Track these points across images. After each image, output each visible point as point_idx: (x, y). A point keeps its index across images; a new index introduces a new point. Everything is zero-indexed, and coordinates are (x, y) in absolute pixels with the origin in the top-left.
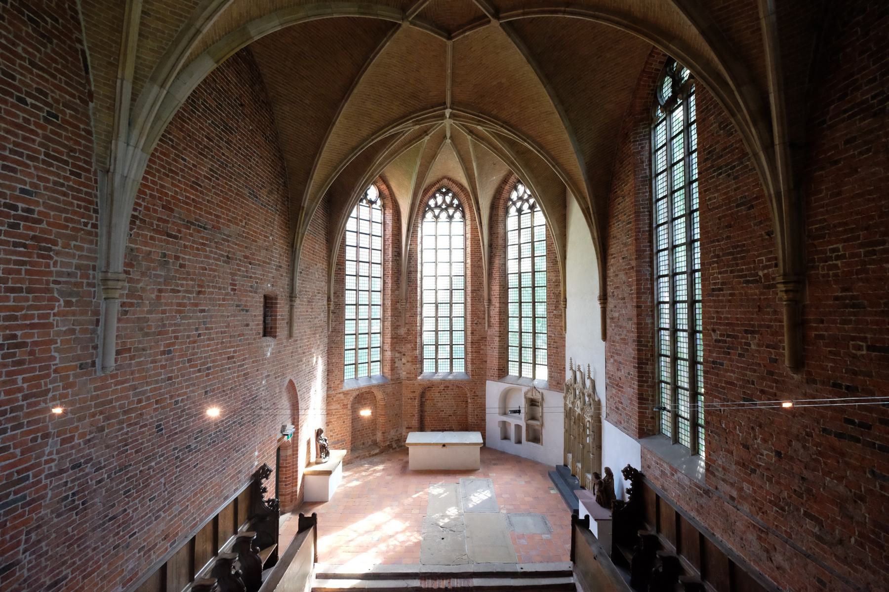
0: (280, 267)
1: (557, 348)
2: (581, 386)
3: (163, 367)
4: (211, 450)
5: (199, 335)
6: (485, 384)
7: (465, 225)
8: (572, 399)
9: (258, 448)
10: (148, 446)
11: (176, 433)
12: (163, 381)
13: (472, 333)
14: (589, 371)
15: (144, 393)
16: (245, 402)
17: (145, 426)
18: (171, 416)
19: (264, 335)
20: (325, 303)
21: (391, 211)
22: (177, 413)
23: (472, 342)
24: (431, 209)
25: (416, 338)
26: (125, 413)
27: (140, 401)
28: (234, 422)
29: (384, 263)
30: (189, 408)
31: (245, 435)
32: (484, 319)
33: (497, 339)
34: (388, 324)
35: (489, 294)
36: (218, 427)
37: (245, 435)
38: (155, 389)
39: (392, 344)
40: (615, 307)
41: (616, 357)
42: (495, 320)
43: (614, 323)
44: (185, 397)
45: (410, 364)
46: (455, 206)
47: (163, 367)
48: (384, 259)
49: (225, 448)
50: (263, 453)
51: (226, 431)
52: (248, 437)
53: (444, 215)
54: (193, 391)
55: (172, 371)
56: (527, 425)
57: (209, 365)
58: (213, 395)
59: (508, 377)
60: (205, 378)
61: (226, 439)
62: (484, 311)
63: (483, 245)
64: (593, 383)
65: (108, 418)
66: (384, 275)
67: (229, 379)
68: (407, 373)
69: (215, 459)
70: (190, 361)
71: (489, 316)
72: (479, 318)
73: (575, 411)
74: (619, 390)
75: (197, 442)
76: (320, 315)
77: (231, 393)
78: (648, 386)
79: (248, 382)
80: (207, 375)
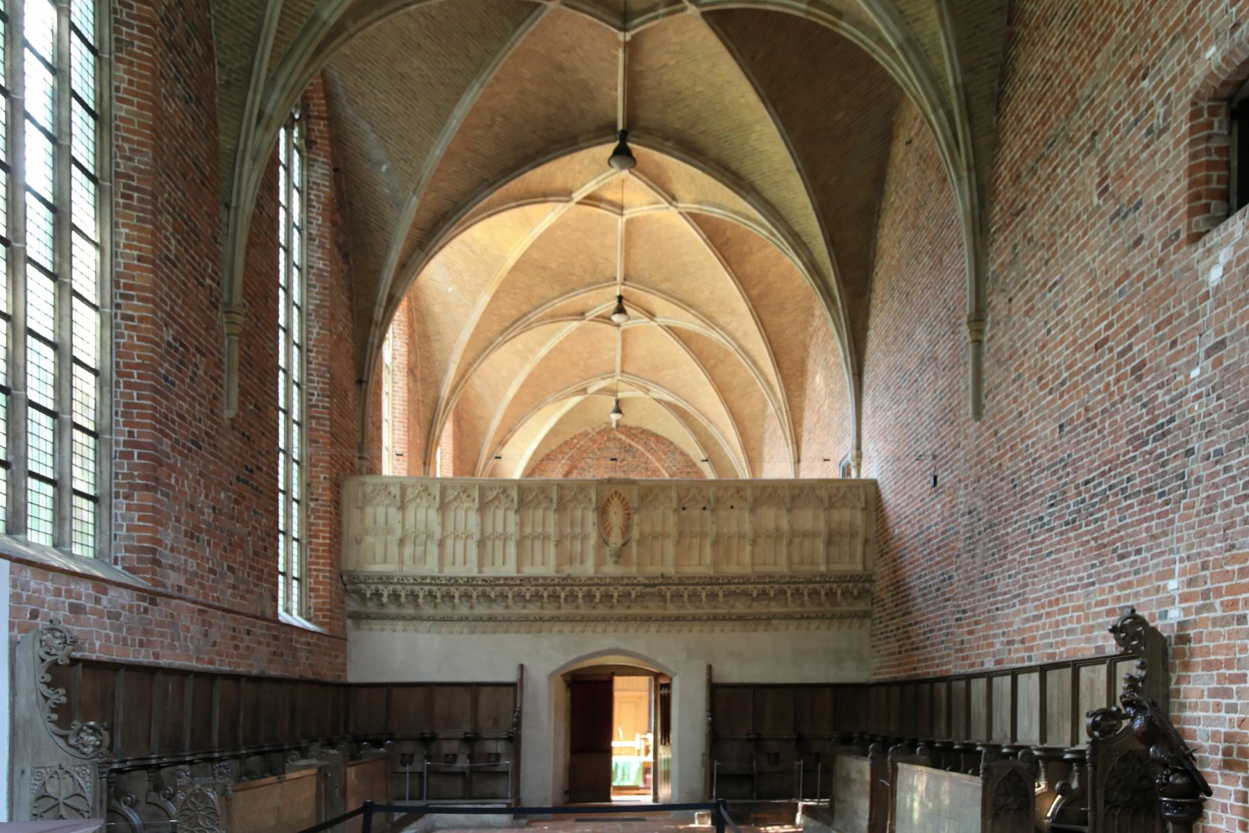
16: (1138, 441)
28: (1111, 488)
30: (1040, 457)
49: (1096, 539)
51: (1093, 505)
77: (1103, 421)
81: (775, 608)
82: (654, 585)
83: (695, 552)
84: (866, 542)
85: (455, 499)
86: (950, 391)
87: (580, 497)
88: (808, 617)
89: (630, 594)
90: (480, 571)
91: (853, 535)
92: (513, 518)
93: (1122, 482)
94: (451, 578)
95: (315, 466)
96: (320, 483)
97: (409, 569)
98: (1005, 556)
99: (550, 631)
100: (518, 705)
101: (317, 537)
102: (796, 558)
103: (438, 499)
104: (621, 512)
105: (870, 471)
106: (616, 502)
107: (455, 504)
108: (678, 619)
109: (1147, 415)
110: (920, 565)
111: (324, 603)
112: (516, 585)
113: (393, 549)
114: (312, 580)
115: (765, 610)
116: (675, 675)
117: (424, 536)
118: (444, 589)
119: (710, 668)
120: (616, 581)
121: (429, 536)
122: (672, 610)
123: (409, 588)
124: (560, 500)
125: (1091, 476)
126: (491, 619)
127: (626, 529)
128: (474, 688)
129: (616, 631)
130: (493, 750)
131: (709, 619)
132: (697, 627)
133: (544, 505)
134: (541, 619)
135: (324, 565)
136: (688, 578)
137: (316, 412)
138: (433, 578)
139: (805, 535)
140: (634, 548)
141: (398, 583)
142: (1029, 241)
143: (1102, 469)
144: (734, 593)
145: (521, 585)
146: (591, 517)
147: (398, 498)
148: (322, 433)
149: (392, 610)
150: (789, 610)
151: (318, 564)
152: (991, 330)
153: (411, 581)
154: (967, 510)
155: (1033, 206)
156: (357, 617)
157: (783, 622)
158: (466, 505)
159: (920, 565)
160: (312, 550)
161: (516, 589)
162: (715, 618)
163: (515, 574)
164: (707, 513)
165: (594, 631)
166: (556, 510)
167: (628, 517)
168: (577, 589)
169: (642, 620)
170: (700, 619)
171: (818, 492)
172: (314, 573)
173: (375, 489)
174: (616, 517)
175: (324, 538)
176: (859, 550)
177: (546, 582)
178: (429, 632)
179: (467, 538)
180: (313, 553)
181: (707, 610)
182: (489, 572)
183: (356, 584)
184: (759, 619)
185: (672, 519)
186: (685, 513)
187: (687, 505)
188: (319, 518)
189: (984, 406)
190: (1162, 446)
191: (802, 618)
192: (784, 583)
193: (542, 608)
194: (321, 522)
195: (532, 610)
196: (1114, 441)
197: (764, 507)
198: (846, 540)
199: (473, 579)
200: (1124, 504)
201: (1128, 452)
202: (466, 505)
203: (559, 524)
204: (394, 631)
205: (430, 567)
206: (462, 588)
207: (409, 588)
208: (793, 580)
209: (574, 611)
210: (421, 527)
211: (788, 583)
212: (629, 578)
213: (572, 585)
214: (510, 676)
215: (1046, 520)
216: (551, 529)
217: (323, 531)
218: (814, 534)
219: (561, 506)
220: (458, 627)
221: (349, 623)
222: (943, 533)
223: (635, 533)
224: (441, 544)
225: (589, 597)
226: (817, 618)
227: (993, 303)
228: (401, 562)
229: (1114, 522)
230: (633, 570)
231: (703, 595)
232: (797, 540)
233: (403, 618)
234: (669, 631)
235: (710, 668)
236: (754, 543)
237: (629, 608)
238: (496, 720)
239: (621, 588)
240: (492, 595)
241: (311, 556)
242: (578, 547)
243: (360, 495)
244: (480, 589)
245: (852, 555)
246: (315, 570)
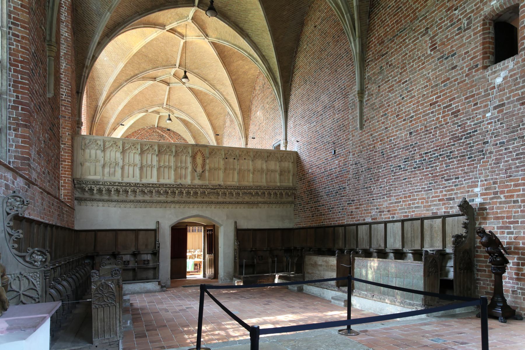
10: (378, 162)
11: (392, 157)
12: (383, 130)
15: (375, 137)
17: (376, 152)
18: (388, 148)
26: (369, 145)
27: (373, 141)
38: (380, 134)
44: (396, 137)
54: (400, 133)
55: (388, 124)
60: (409, 124)
65: (363, 148)
70: (397, 116)
75: (405, 165)
80: (411, 122)
81: (260, 199)
82: (215, 189)
83: (231, 176)
84: (293, 175)
85: (129, 148)
86: (343, 119)
87: (185, 151)
88: (272, 203)
89: (205, 192)
90: (141, 181)
91: (289, 172)
92: (155, 158)
94: (127, 183)
95: (64, 128)
96: (67, 136)
97: (107, 178)
98: (378, 180)
99: (170, 207)
100: (157, 239)
101: (65, 162)
102: (269, 180)
103: (121, 148)
104: (201, 158)
105: (293, 147)
106: (199, 154)
107: (129, 151)
108: (223, 203)
110: (326, 183)
111: (68, 193)
112: (157, 187)
113: (99, 169)
114: (62, 182)
115: (256, 200)
116: (221, 225)
117: (114, 164)
118: (124, 188)
119: (236, 223)
120: (201, 186)
121: (117, 164)
122: (221, 199)
123: (107, 187)
124: (176, 152)
126: (144, 202)
127: (203, 166)
128: (136, 231)
129: (198, 207)
130: (146, 259)
131: (235, 203)
132: (230, 206)
133: (169, 154)
134: (167, 202)
135: (68, 174)
136: (229, 186)
137: (64, 103)
138: (119, 183)
139: (272, 171)
140: (207, 174)
141: (102, 185)
142: (390, 66)
144: (246, 193)
145: (159, 187)
146: (189, 160)
147: (102, 146)
148: (67, 113)
149: (98, 197)
150: (265, 200)
151: (65, 174)
152: (368, 97)
153: (109, 184)
154: (354, 163)
155: (392, 53)
156: (80, 200)
157: (263, 205)
158: (134, 151)
159: (326, 183)
160: (62, 167)
161: (156, 189)
162: (238, 203)
163: (157, 182)
164: (236, 161)
165: (189, 208)
166: (174, 156)
167: (204, 161)
168: (183, 189)
169: (209, 203)
170: (232, 203)
171: (276, 155)
172: (63, 178)
173: (90, 141)
174: (199, 160)
175: (68, 162)
176: (291, 178)
177: (170, 186)
178: (115, 207)
179: (134, 166)
180: (63, 169)
181: (234, 199)
182: (144, 181)
183: (81, 184)
184: (254, 203)
185: (222, 162)
186: (227, 160)
187: (228, 157)
188: (66, 153)
189: (364, 125)
191: (270, 203)
192: (265, 190)
193: (167, 197)
194: (67, 154)
195: (163, 198)
197: (257, 160)
198: (286, 174)
199: (138, 184)
202: (134, 151)
203: (176, 162)
204: (98, 206)
205: (117, 178)
206: (132, 188)
207: (107, 187)
208: (268, 188)
209: (180, 199)
210: (113, 160)
211: (267, 189)
212: (205, 186)
213: (181, 188)
214: (153, 226)
215: (402, 167)
216: (172, 164)
217: (68, 159)
218: (275, 171)
219: (177, 154)
220: (128, 205)
221: (76, 202)
222: (339, 172)
223: (207, 167)
224: (123, 168)
225: (188, 193)
226: (275, 203)
227: (369, 87)
228: (103, 175)
230: (207, 183)
231: (234, 193)
232: (269, 173)
233: (103, 200)
234: (219, 208)
235: (236, 223)
236: (253, 174)
237: (203, 198)
238: (146, 246)
239: (201, 190)
240: (146, 191)
241: (62, 170)
242: (183, 172)
243: (83, 144)
244: (140, 188)
245: (289, 179)
246: (64, 177)
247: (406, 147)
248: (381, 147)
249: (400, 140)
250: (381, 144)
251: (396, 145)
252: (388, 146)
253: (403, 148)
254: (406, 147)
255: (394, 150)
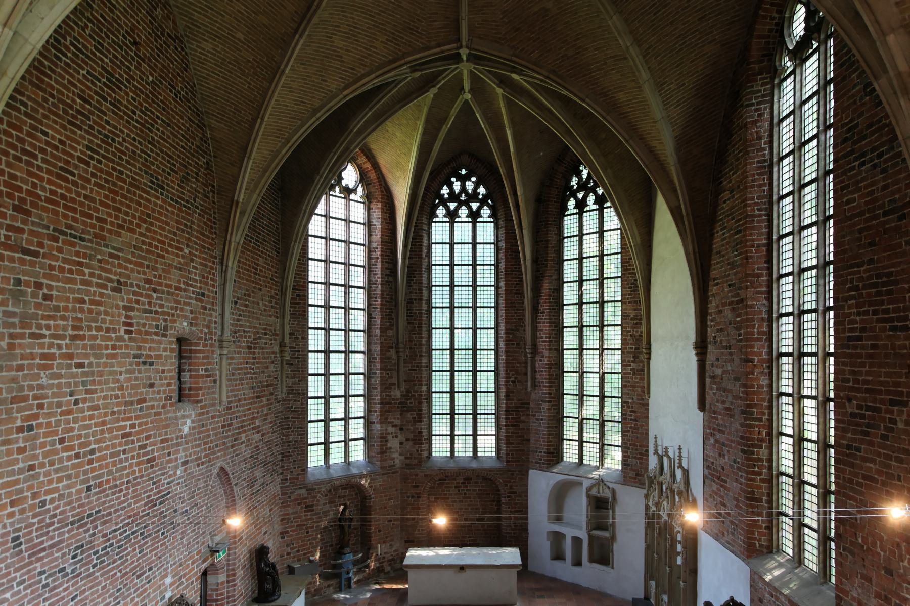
0: (203, 295)
1: (636, 420)
2: (669, 479)
3: (21, 450)
4: (97, 574)
5: (76, 402)
6: (527, 472)
7: (497, 228)
8: (656, 499)
9: (172, 571)
12: (21, 471)
13: (507, 396)
14: (680, 456)
16: (151, 504)
18: (34, 524)
19: (180, 401)
20: (277, 349)
21: (379, 205)
22: (43, 520)
23: (506, 411)
24: (444, 202)
25: (420, 403)
28: (133, 533)
29: (370, 287)
31: (151, 551)
32: (526, 374)
33: (545, 406)
34: (376, 381)
35: (534, 337)
36: (109, 540)
37: (151, 551)
39: (383, 413)
40: (718, 359)
41: (718, 436)
42: (543, 376)
43: (715, 383)
44: (56, 495)
45: (411, 443)
46: (480, 197)
47: (21, 450)
48: (369, 281)
50: (180, 578)
52: (155, 555)
53: (463, 212)
54: (68, 487)
55: (35, 457)
56: (591, 538)
57: (93, 446)
58: (100, 492)
59: (562, 464)
60: (87, 467)
61: (121, 558)
62: (526, 363)
63: (525, 259)
64: (686, 473)
66: (369, 305)
67: (125, 468)
68: (406, 458)
69: (103, 588)
71: (534, 371)
72: (517, 373)
73: (659, 516)
74: (722, 486)
76: (267, 367)
77: (128, 488)
78: (762, 481)
79: (154, 472)
80: (90, 462)
93: (141, 529)
109: (156, 489)
125: (118, 527)
143: (127, 521)
190: (163, 507)
196: (136, 503)
200: (142, 542)
201: (145, 510)
229: (136, 555)
247: (79, 520)
248: (12, 524)
249: (65, 504)
250: (10, 515)
251: (55, 516)
252: (35, 520)
253: (72, 523)
254: (79, 520)
255: (51, 528)
